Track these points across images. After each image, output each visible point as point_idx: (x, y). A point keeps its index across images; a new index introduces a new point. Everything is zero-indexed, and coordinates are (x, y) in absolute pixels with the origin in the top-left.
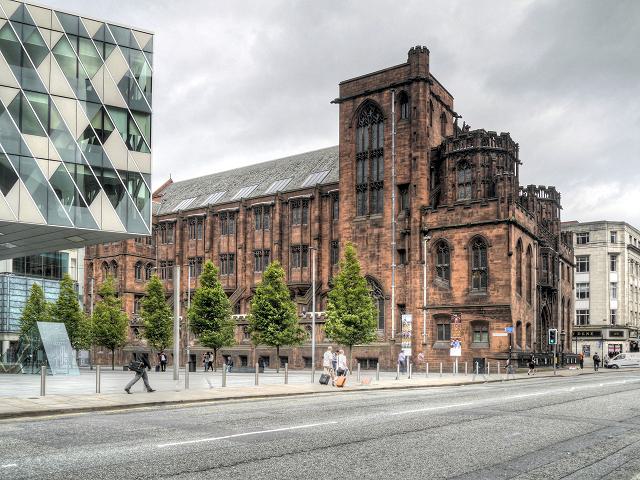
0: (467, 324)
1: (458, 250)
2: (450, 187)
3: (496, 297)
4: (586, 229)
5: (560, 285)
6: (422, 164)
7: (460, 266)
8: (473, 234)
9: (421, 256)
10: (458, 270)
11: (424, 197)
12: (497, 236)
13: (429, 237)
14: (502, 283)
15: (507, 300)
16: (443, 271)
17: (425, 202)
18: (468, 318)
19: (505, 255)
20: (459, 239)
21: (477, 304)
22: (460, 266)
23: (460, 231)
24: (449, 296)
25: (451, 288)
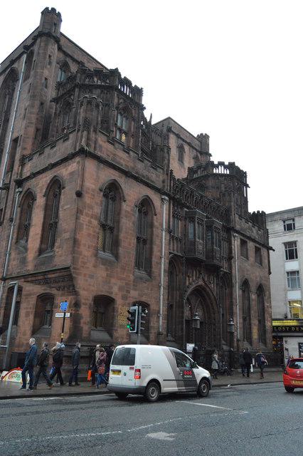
0: (33, 301)
1: (40, 201)
2: (54, 133)
3: (61, 257)
4: (291, 216)
5: (236, 264)
6: (31, 113)
7: (38, 218)
8: (52, 176)
9: (12, 213)
10: (35, 225)
11: (27, 146)
12: (72, 174)
13: (20, 190)
14: (67, 235)
15: (68, 263)
16: (24, 230)
17: (27, 152)
18: (38, 289)
19: (75, 196)
20: (40, 185)
21: (44, 269)
22: (38, 218)
23: (44, 175)
24: (23, 261)
25: (26, 249)
